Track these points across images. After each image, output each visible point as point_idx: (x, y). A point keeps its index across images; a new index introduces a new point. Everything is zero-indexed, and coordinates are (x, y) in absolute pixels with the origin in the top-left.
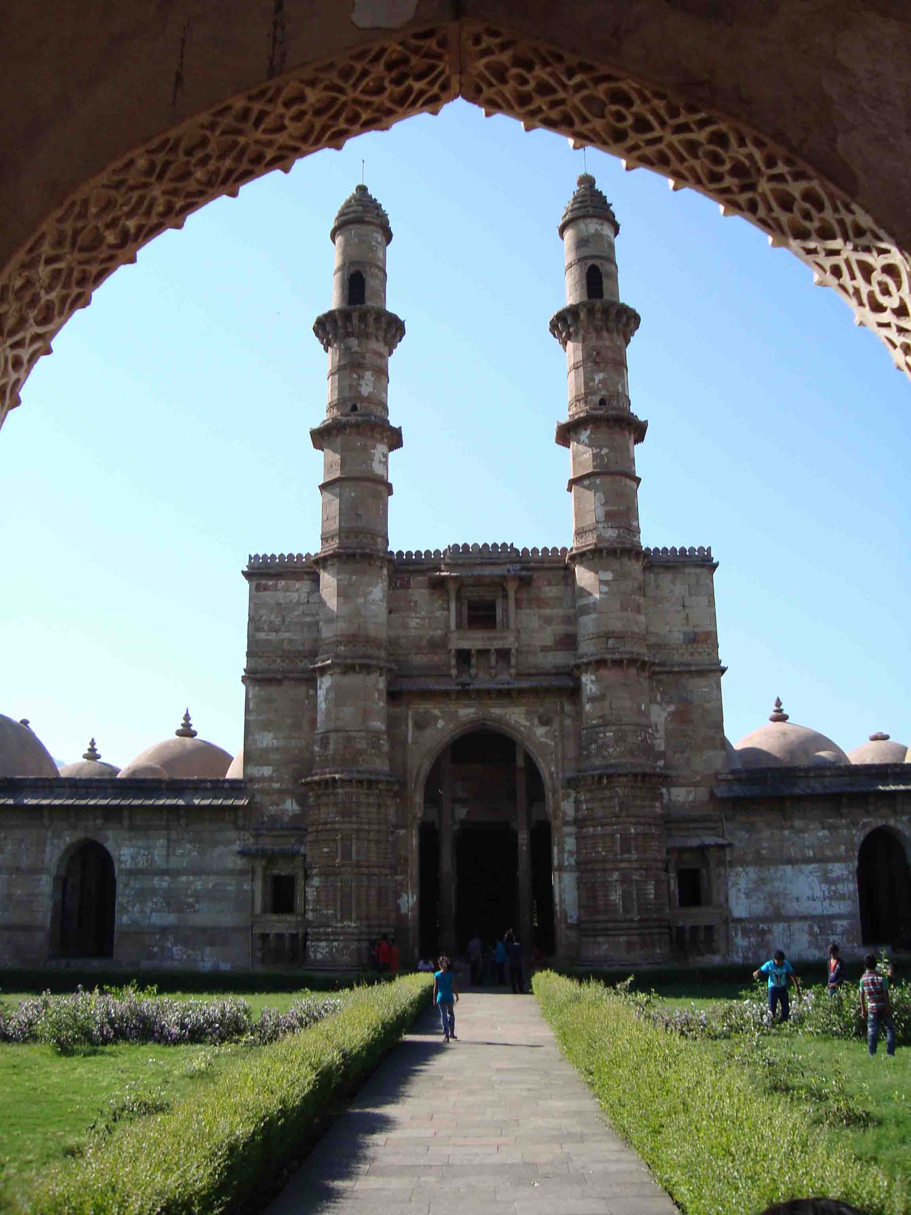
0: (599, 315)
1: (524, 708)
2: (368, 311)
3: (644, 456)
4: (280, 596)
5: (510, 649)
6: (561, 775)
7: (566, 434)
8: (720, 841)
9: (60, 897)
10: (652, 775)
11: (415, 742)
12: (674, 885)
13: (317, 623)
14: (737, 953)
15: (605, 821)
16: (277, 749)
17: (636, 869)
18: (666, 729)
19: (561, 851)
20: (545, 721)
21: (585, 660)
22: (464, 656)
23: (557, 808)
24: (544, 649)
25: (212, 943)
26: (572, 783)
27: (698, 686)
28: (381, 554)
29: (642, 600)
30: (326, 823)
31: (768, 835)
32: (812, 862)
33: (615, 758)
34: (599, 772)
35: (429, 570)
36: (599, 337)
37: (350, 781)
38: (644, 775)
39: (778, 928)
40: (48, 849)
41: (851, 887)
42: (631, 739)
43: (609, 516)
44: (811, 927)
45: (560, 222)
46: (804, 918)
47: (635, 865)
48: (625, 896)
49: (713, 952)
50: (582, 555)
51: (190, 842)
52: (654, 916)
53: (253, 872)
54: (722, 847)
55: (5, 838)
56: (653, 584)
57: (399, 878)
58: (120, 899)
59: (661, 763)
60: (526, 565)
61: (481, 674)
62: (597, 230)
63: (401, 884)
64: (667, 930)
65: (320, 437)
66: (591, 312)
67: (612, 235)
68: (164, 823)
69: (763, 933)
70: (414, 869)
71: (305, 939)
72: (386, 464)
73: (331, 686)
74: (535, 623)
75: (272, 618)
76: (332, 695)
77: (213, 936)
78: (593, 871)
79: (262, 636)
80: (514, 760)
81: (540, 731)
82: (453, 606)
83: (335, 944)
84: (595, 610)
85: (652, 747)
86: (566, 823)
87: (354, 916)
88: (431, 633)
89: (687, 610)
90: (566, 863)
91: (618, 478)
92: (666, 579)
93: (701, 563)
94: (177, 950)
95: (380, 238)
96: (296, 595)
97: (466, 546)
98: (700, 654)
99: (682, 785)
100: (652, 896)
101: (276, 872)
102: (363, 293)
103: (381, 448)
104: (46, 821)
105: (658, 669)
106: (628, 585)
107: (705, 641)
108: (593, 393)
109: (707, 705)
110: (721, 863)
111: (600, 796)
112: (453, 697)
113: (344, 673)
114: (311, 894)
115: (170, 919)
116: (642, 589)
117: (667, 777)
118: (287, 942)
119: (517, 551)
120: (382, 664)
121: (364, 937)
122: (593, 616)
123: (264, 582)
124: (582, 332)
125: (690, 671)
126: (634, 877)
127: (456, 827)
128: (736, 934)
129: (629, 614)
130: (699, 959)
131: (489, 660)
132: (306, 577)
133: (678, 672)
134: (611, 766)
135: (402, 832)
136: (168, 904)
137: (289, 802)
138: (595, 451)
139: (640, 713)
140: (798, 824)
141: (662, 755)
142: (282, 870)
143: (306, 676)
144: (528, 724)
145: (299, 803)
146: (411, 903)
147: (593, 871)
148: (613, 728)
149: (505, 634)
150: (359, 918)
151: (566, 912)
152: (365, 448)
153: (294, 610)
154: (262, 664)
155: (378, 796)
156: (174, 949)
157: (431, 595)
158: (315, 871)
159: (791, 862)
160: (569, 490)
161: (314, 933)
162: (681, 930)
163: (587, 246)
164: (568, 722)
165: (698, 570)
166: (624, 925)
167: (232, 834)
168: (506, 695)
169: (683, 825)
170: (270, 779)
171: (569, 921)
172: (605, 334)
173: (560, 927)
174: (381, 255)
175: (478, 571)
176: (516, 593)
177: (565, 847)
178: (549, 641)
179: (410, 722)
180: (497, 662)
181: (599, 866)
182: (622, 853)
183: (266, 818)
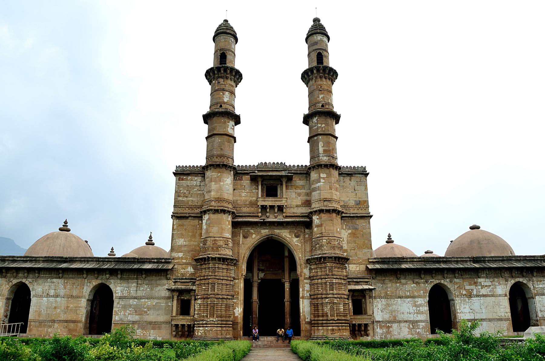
0: (321, 71)
2: (228, 67)
3: (339, 129)
4: (189, 182)
7: (307, 120)
8: (371, 287)
9: (90, 308)
10: (342, 258)
17: (336, 298)
21: (314, 210)
22: (264, 208)
24: (297, 206)
25: (154, 329)
26: (308, 261)
27: (360, 223)
31: (391, 286)
36: (321, 80)
37: (215, 258)
39: (395, 326)
40: (85, 288)
41: (426, 308)
43: (325, 151)
45: (306, 36)
46: (406, 321)
47: (335, 296)
48: (332, 309)
49: (367, 335)
50: (314, 167)
53: (173, 298)
54: (371, 290)
55: (67, 283)
57: (235, 301)
58: (114, 309)
59: (345, 254)
61: (271, 216)
63: (235, 303)
65: (207, 118)
66: (318, 70)
69: (389, 327)
70: (241, 297)
72: (233, 129)
74: (293, 195)
77: (155, 325)
78: (318, 298)
79: (181, 198)
81: (295, 240)
82: (260, 187)
83: (207, 328)
85: (342, 246)
86: (305, 279)
88: (251, 198)
91: (329, 136)
92: (347, 179)
94: (139, 332)
95: (233, 40)
96: (195, 182)
97: (266, 163)
98: (362, 209)
99: (354, 264)
103: (232, 123)
104: (85, 276)
105: (344, 215)
108: (319, 102)
110: (370, 297)
112: (259, 225)
115: (137, 318)
116: (338, 181)
117: (348, 259)
118: (186, 329)
122: (318, 192)
124: (314, 78)
125: (357, 217)
130: (361, 338)
133: (353, 217)
134: (325, 254)
135: (237, 281)
136: (136, 312)
138: (319, 125)
139: (337, 232)
140: (403, 281)
141: (346, 251)
142: (186, 297)
147: (318, 298)
148: (326, 238)
149: (283, 199)
150: (217, 317)
152: (225, 123)
154: (180, 210)
155: (227, 265)
156: (138, 331)
157: (251, 183)
158: (199, 297)
159: (400, 297)
160: (308, 142)
164: (307, 236)
165: (361, 176)
167: (165, 281)
168: (280, 224)
169: (355, 280)
170: (182, 258)
171: (307, 320)
172: (324, 79)
173: (302, 323)
174: (233, 47)
175: (270, 174)
177: (305, 289)
178: (299, 203)
179: (241, 235)
181: (319, 296)
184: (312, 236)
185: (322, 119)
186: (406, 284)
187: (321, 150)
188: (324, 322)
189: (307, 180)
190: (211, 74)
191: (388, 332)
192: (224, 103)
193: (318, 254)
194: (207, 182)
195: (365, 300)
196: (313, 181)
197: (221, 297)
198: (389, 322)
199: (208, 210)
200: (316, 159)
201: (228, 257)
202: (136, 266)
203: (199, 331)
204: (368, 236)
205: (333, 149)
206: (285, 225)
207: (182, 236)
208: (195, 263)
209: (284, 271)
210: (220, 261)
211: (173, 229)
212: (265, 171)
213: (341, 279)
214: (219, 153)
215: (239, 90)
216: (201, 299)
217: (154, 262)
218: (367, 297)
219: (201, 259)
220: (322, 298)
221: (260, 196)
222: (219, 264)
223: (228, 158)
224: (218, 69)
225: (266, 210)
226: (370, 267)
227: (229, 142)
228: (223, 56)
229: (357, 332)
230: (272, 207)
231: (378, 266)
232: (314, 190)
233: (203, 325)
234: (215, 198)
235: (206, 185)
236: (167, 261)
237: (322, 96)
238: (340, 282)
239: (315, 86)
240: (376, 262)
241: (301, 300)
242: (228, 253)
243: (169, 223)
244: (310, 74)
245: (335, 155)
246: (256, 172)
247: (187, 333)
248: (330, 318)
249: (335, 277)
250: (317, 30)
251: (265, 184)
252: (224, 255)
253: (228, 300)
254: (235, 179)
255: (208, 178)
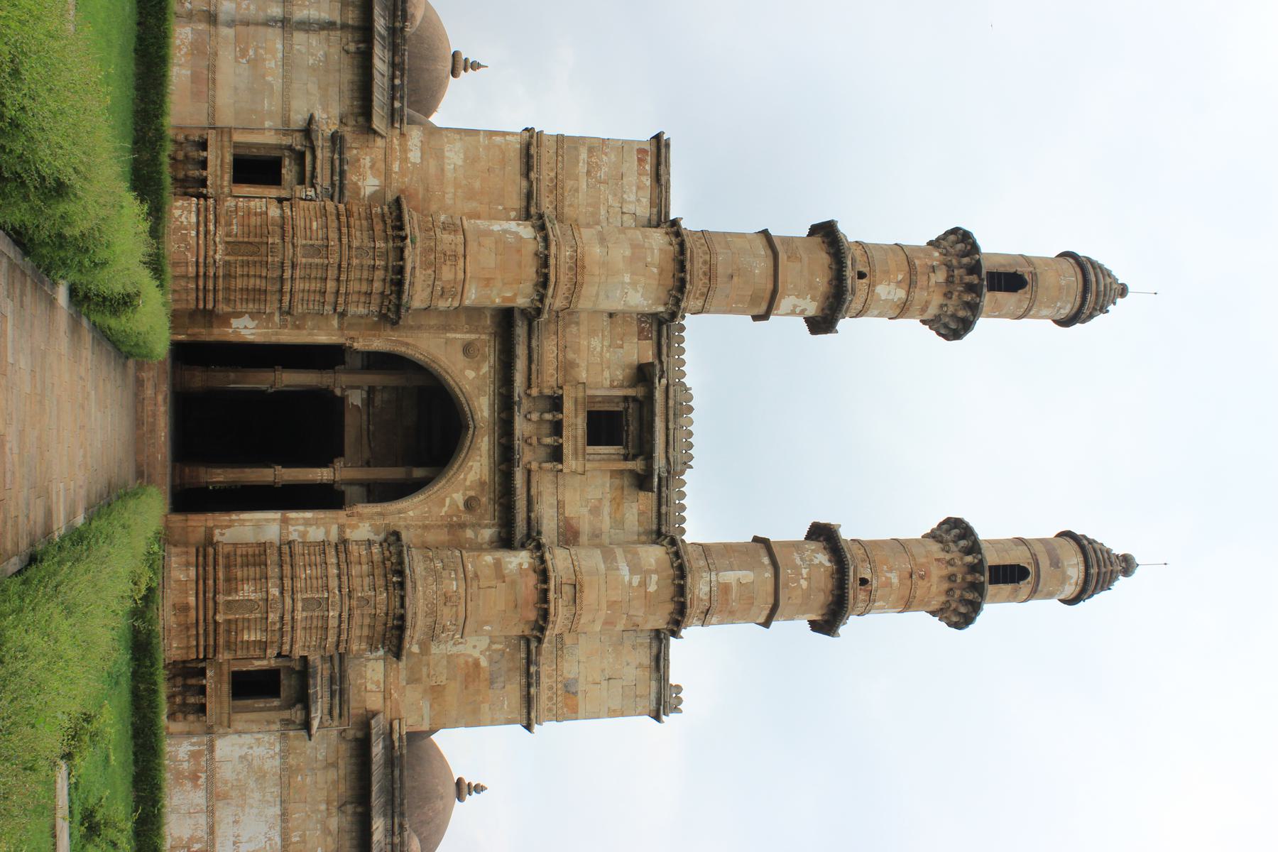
0: (969, 578)
1: (486, 477)
2: (980, 295)
3: (794, 631)
4: (631, 179)
5: (561, 462)
6: (402, 523)
7: (823, 534)
8: (315, 724)
10: (401, 639)
11: (447, 341)
12: (259, 664)
13: (598, 223)
14: (170, 745)
15: (345, 578)
16: (443, 170)
17: (282, 618)
18: (458, 656)
19: (307, 523)
20: (469, 504)
21: (547, 556)
22: (556, 403)
23: (360, 516)
24: (560, 505)
26: (394, 537)
28: (683, 305)
29: (620, 627)
30: (348, 227)
32: (283, 840)
33: (424, 593)
34: (407, 571)
35: (661, 362)
36: (942, 577)
37: (402, 258)
38: (400, 628)
39: (199, 798)
42: (446, 615)
43: (726, 588)
44: (199, 840)
45: (1078, 533)
46: (211, 831)
47: (287, 617)
48: (248, 605)
50: (677, 555)
51: (326, 55)
52: (221, 641)
53: (287, 132)
54: (306, 725)
56: (639, 640)
57: (277, 318)
60: (664, 483)
62: (1071, 578)
64: (201, 656)
65: (826, 232)
67: (1062, 597)
68: (350, 22)
69: (194, 778)
70: (288, 336)
71: (199, 196)
72: (793, 313)
73: (521, 238)
75: (605, 169)
76: (511, 239)
77: (206, 79)
79: (584, 155)
80: (419, 464)
81: (459, 498)
83: (193, 233)
84: (607, 569)
86: (341, 528)
87: (227, 258)
88: (583, 365)
89: (605, 683)
90: (291, 528)
91: (771, 600)
93: (663, 703)
95: (1066, 311)
96: (633, 198)
97: (691, 409)
98: (550, 699)
100: (246, 637)
101: (287, 162)
102: (1000, 290)
103: (812, 308)
105: (533, 645)
106: (639, 612)
107: (566, 705)
109: (485, 707)
110: (287, 723)
111: (376, 572)
113: (536, 254)
114: (256, 205)
116: (635, 628)
117: (398, 656)
119: (682, 473)
120: (547, 302)
121: (202, 270)
122: (602, 567)
123: (649, 159)
124: (948, 557)
125: (529, 685)
126: (271, 616)
127: (338, 392)
128: (193, 744)
129: (604, 612)
131: (550, 436)
132: (655, 210)
134: (415, 587)
135: (335, 323)
137: (376, 182)
138: (804, 572)
140: (333, 823)
141: (425, 648)
143: (533, 210)
144: (468, 483)
145: (373, 196)
146: (243, 332)
148: (462, 591)
151: (229, 527)
152: (812, 287)
153: (615, 195)
155: (382, 293)
159: (284, 816)
160: (756, 539)
161: (206, 209)
162: (202, 673)
163: (1051, 565)
165: (653, 697)
166: (211, 604)
167: (335, 111)
168: (506, 456)
170: (405, 160)
171: (217, 531)
172: (946, 586)
174: (1045, 312)
176: (631, 471)
177: (309, 526)
178: (570, 511)
179: (473, 336)
180: (548, 446)
182: (303, 599)
183: (355, 152)
184: (471, 549)
185: (824, 582)
186: (326, 831)
187: (730, 577)
188: (211, 582)
189: (639, 534)
190: (960, 246)
191: (179, 776)
192: (871, 286)
193: (417, 566)
194: (630, 233)
195: (280, 708)
196: (636, 554)
197: (287, 274)
198: (211, 778)
199: (546, 239)
200: (702, 563)
201: (405, 298)
202: (380, 24)
203: (182, 212)
204: (473, 718)
205: (732, 613)
206: (503, 467)
207: (471, 160)
208: (390, 197)
209: (368, 464)
210: (395, 273)
211: (491, 134)
212: (667, 408)
213: (339, 637)
214: (720, 270)
215: (913, 331)
216: (283, 217)
217: (393, 77)
218: (286, 714)
219: (400, 217)
220: (282, 579)
221: (590, 392)
222: (386, 268)
223: (706, 296)
224: (975, 268)
225: (550, 411)
226: (377, 726)
227: (754, 301)
228: (1011, 281)
229: (179, 681)
230: (557, 428)
231: (377, 749)
232: (608, 556)
233: (202, 222)
234: (582, 260)
235: (623, 229)
236: (397, 117)
237: (895, 581)
238: (331, 632)
239: (923, 560)
240: (392, 742)
241: (276, 515)
242: (418, 297)
243: (511, 119)
244: (962, 543)
245: (714, 620)
246: (664, 381)
247: (181, 175)
248: (221, 598)
249: (345, 615)
250: (1098, 569)
251: (626, 409)
252: (412, 284)
253: (277, 296)
254: (643, 317)
255: (645, 237)
